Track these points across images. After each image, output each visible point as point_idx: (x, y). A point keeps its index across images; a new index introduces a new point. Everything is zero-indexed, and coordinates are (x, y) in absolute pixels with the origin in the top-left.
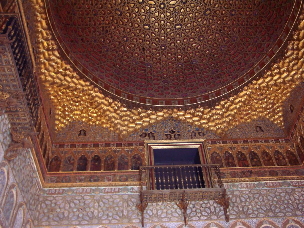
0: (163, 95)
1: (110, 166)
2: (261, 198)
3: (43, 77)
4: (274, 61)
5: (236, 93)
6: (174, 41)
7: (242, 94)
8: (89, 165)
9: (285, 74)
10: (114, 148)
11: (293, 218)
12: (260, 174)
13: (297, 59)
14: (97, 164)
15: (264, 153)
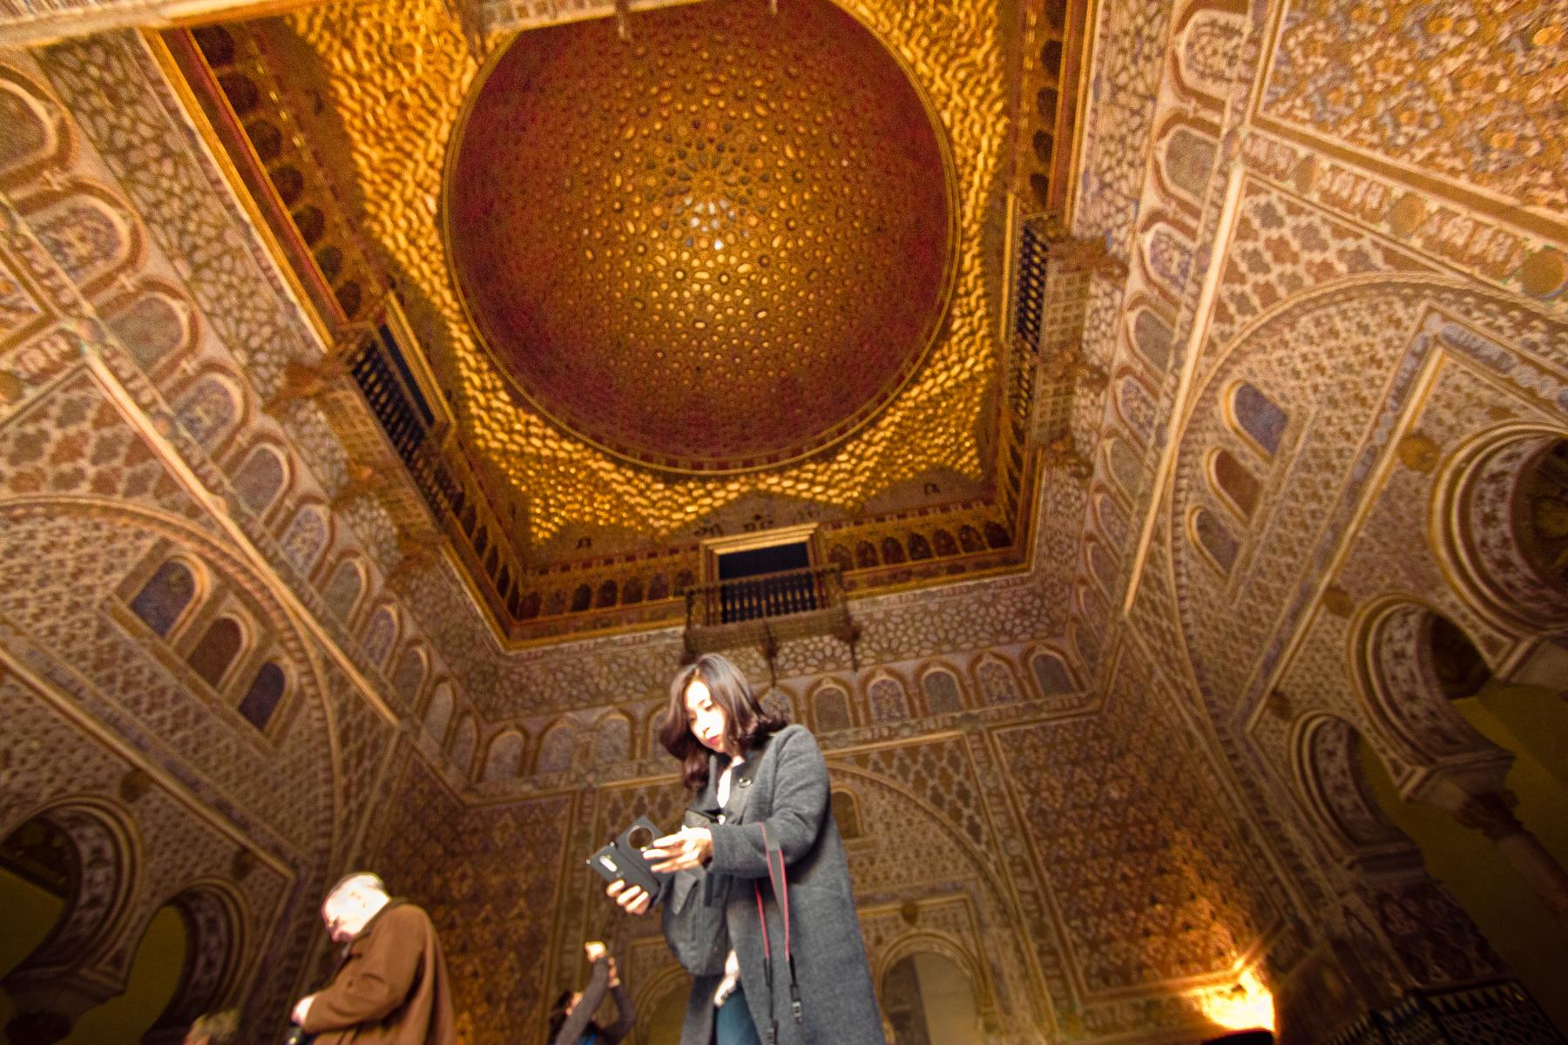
0: (737, 450)
1: (633, 596)
2: (927, 620)
3: (480, 443)
4: (935, 347)
5: (874, 424)
6: (757, 343)
7: (884, 423)
8: (594, 600)
9: (957, 369)
10: (640, 562)
11: (996, 649)
12: (928, 574)
13: (973, 333)
14: (609, 594)
15: (940, 534)
